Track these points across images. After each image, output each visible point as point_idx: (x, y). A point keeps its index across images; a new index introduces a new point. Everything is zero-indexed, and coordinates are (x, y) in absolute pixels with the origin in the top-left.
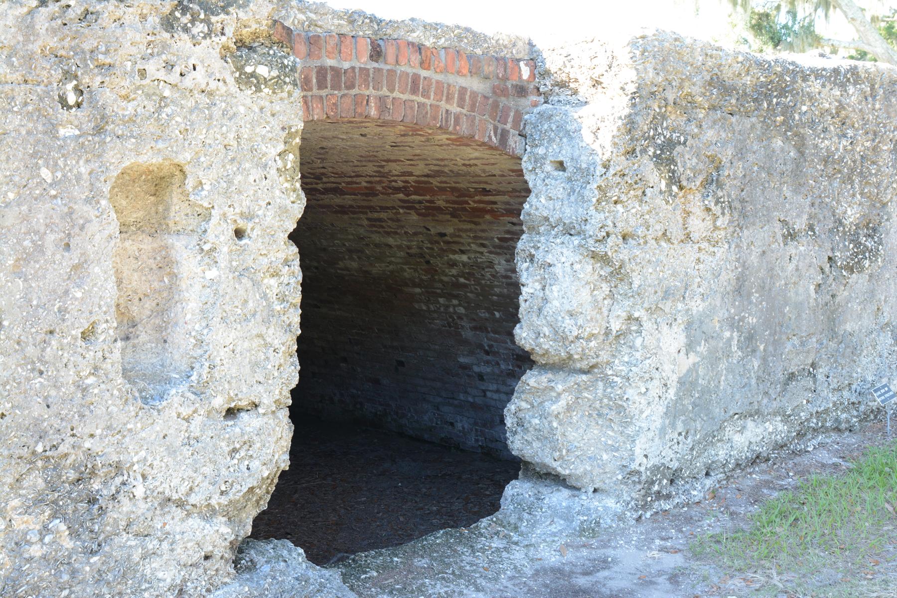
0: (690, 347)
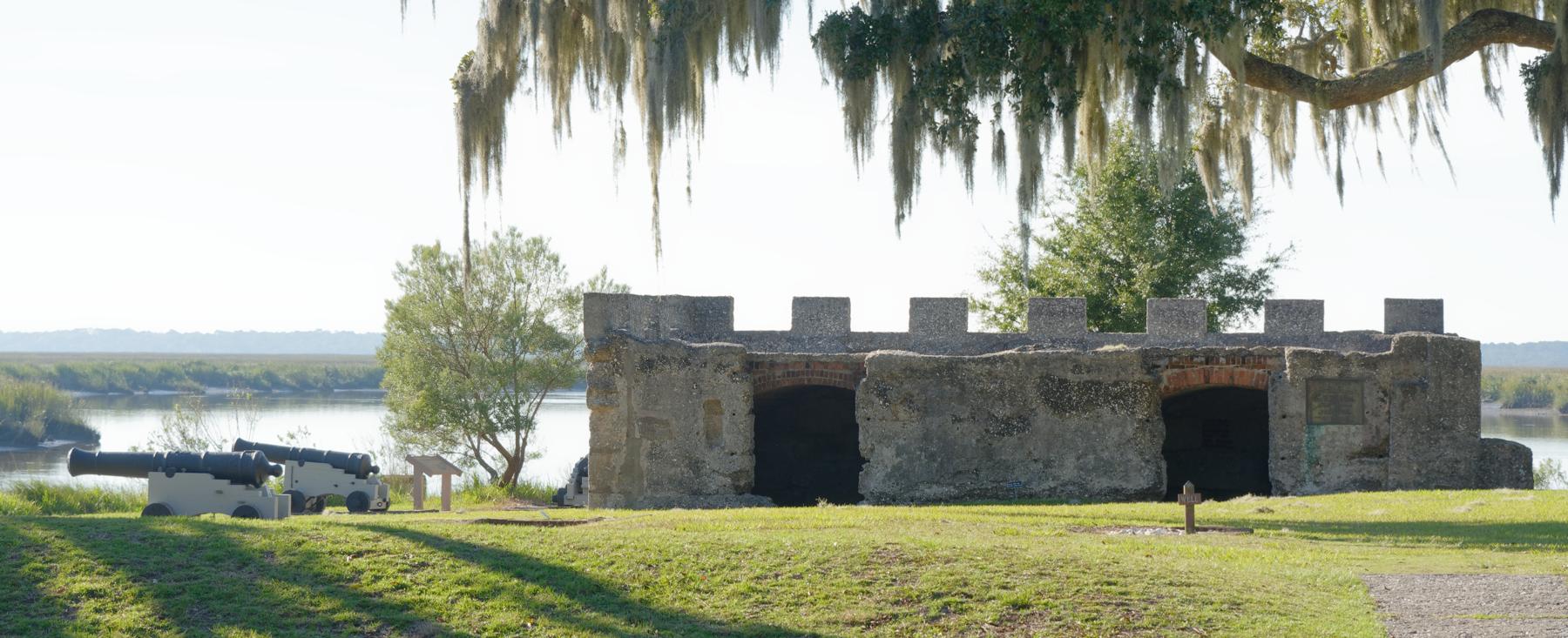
0: (898, 455)
